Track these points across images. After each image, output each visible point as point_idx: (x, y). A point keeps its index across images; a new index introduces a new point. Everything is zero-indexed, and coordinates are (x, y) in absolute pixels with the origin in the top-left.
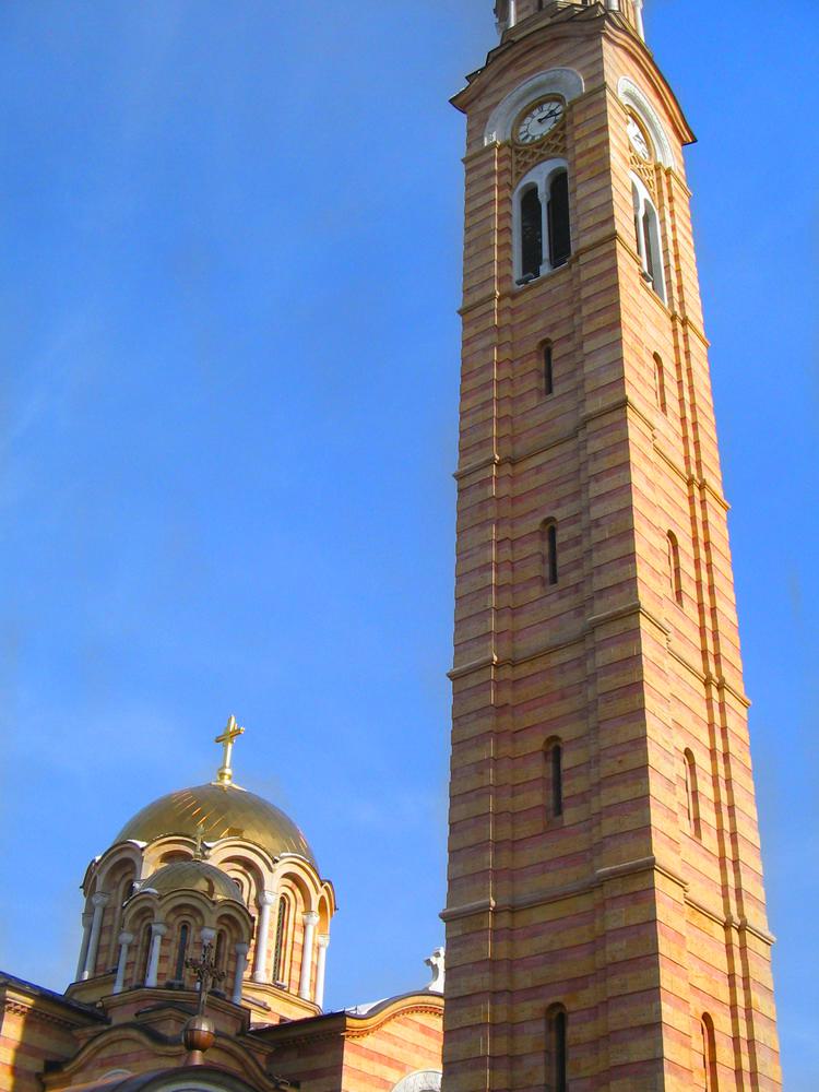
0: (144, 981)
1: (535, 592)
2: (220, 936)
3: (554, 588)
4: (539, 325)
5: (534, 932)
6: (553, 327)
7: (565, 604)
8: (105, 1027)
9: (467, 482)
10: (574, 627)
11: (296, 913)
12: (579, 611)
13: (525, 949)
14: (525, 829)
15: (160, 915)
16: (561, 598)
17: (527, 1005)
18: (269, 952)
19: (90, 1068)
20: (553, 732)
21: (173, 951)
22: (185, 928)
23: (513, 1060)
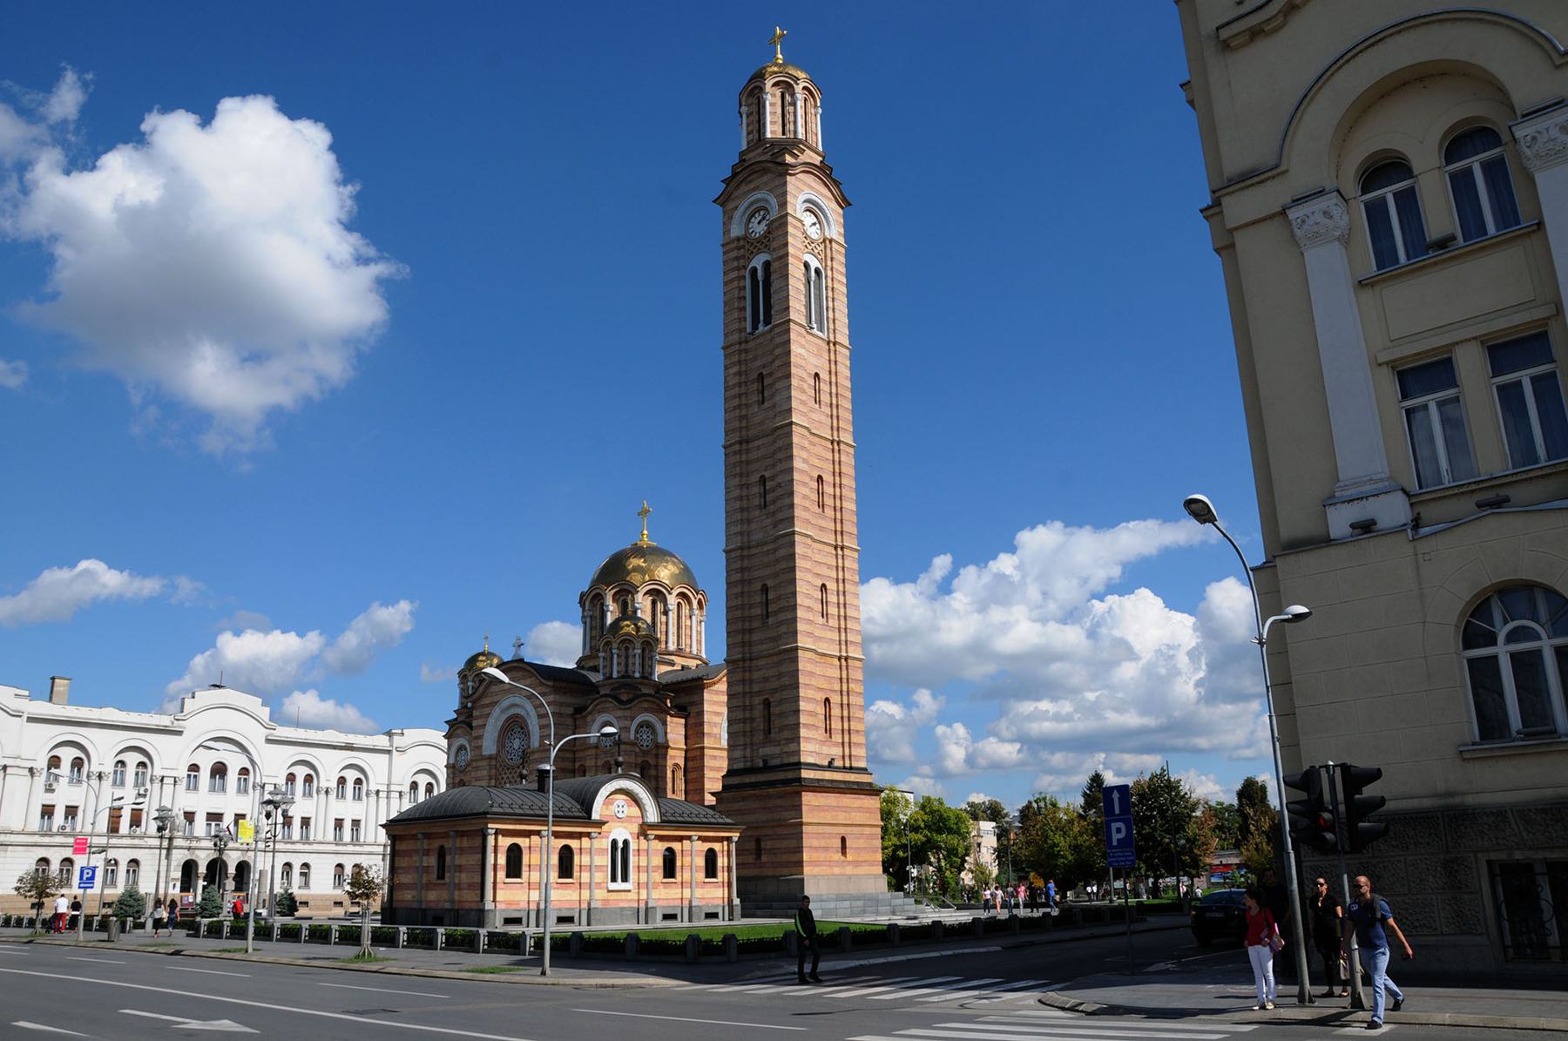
0: (611, 674)
1: (757, 513)
2: (643, 650)
4: (758, 363)
6: (764, 366)
8: (598, 696)
9: (729, 450)
11: (685, 610)
12: (775, 526)
13: (756, 675)
14: (756, 624)
15: (615, 645)
16: (767, 518)
17: (757, 698)
18: (673, 633)
20: (765, 582)
21: (623, 660)
22: (627, 648)
23: (752, 720)
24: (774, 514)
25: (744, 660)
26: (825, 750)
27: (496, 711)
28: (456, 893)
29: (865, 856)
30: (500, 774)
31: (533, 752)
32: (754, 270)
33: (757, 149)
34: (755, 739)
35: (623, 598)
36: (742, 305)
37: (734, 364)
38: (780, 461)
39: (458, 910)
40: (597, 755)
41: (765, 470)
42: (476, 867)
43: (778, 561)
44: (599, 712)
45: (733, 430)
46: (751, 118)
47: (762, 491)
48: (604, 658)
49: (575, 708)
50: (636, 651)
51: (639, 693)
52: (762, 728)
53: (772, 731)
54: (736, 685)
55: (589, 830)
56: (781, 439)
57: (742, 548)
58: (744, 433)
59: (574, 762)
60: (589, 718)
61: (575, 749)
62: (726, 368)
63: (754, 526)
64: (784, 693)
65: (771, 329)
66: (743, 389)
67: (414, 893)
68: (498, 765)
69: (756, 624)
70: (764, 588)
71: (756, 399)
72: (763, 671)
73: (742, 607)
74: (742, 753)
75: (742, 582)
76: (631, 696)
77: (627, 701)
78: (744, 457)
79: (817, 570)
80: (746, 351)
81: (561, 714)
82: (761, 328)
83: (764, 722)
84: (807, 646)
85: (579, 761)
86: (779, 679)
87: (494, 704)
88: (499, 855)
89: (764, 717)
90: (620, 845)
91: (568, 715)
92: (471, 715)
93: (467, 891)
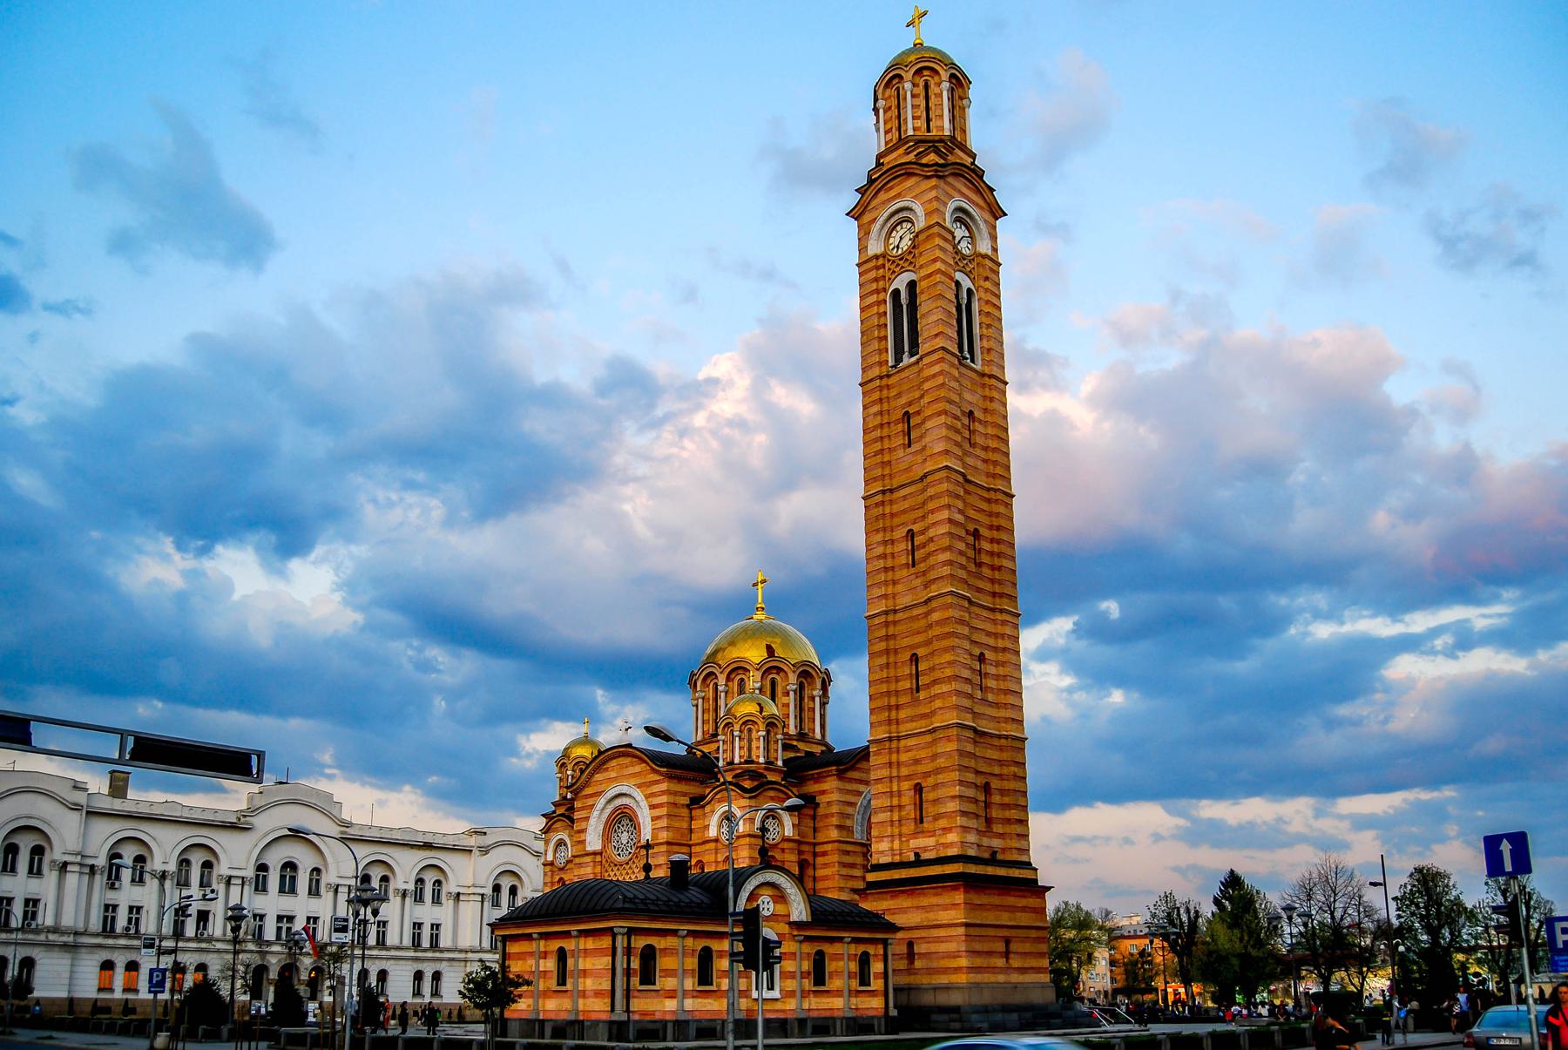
1: (905, 572)
2: (768, 732)
3: (912, 570)
4: (903, 400)
5: (908, 750)
6: (910, 404)
7: (918, 582)
9: (870, 502)
10: (924, 596)
12: (926, 586)
13: (904, 757)
14: (903, 700)
16: (917, 577)
19: (712, 802)
22: (750, 730)
23: (900, 807)
24: (924, 573)
25: (890, 739)
26: (986, 841)
27: (602, 801)
28: (581, 1001)
29: (1033, 963)
30: (606, 871)
34: (905, 830)
35: (739, 677)
36: (882, 334)
37: (874, 403)
38: (932, 511)
39: (583, 1021)
41: (914, 523)
42: (605, 972)
43: (930, 626)
45: (875, 479)
47: (910, 548)
48: (723, 741)
49: (690, 798)
50: (760, 733)
53: (925, 820)
54: (882, 768)
56: (933, 486)
57: (886, 613)
60: (708, 809)
61: (691, 843)
62: (865, 407)
63: (899, 588)
64: (940, 776)
65: (917, 362)
66: (886, 431)
67: (530, 1001)
68: (604, 862)
69: (903, 700)
72: (914, 753)
73: (887, 680)
74: (890, 845)
75: (887, 652)
76: (756, 783)
77: (751, 788)
79: (975, 637)
80: (888, 387)
81: (676, 804)
82: (907, 360)
83: (915, 809)
85: (696, 856)
86: (932, 761)
87: (598, 794)
88: (632, 958)
89: (915, 804)
91: (683, 805)
92: (571, 809)
93: (593, 1000)
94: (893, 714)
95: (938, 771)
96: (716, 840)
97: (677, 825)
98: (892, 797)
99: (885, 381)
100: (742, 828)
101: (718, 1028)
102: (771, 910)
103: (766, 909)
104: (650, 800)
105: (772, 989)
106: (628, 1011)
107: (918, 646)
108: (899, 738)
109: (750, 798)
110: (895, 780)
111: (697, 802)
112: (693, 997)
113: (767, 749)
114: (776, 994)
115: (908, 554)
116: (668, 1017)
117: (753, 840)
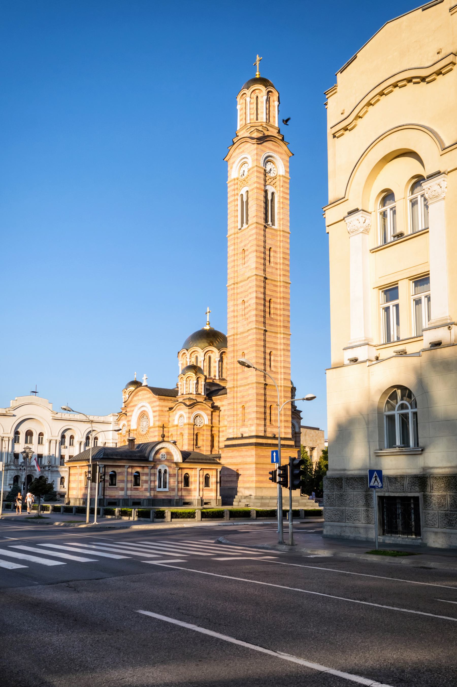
3: (244, 317)
4: (243, 244)
5: (240, 392)
6: (245, 246)
7: (245, 322)
8: (178, 402)
13: (239, 395)
19: (176, 410)
25: (234, 387)
31: (150, 428)
32: (242, 195)
33: (243, 129)
34: (239, 424)
36: (236, 214)
38: (250, 293)
40: (177, 429)
41: (245, 298)
44: (178, 410)
46: (242, 112)
51: (195, 401)
52: (241, 419)
55: (148, 465)
58: (236, 279)
59: (169, 432)
60: (174, 412)
63: (239, 325)
66: (236, 258)
70: (243, 354)
71: (241, 262)
76: (192, 403)
78: (235, 291)
80: (237, 238)
82: (245, 226)
83: (242, 416)
84: (260, 381)
89: (242, 414)
90: (163, 472)
91: (166, 411)
94: (235, 377)
95: (250, 401)
96: (177, 426)
97: (163, 419)
98: (234, 411)
99: (236, 236)
100: (186, 421)
101: (142, 502)
102: (166, 458)
103: (163, 458)
104: (153, 408)
105: (166, 487)
106: (104, 495)
107: (245, 349)
108: (237, 387)
109: (189, 409)
110: (235, 404)
111: (171, 409)
112: (131, 490)
113: (197, 388)
114: (167, 489)
115: (243, 311)
116: (120, 498)
117: (190, 426)
